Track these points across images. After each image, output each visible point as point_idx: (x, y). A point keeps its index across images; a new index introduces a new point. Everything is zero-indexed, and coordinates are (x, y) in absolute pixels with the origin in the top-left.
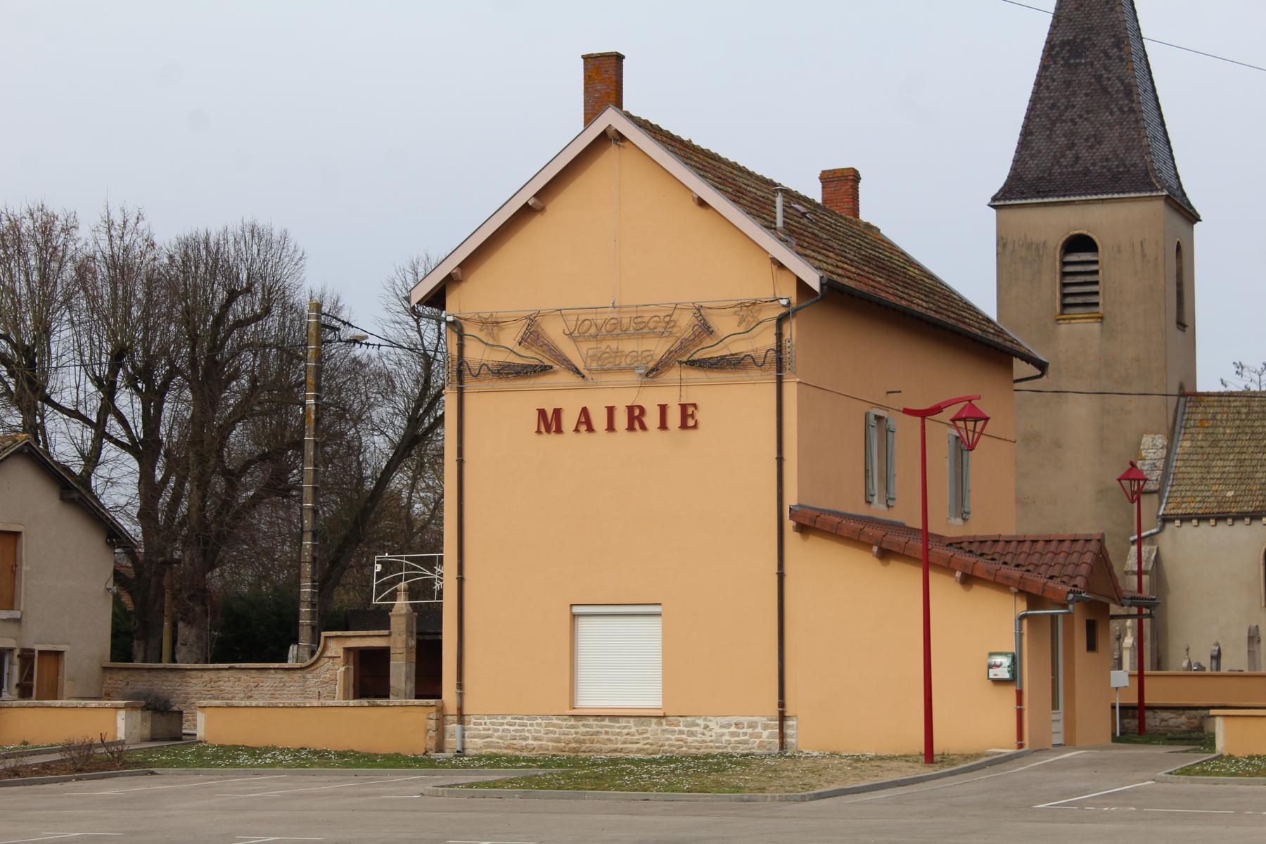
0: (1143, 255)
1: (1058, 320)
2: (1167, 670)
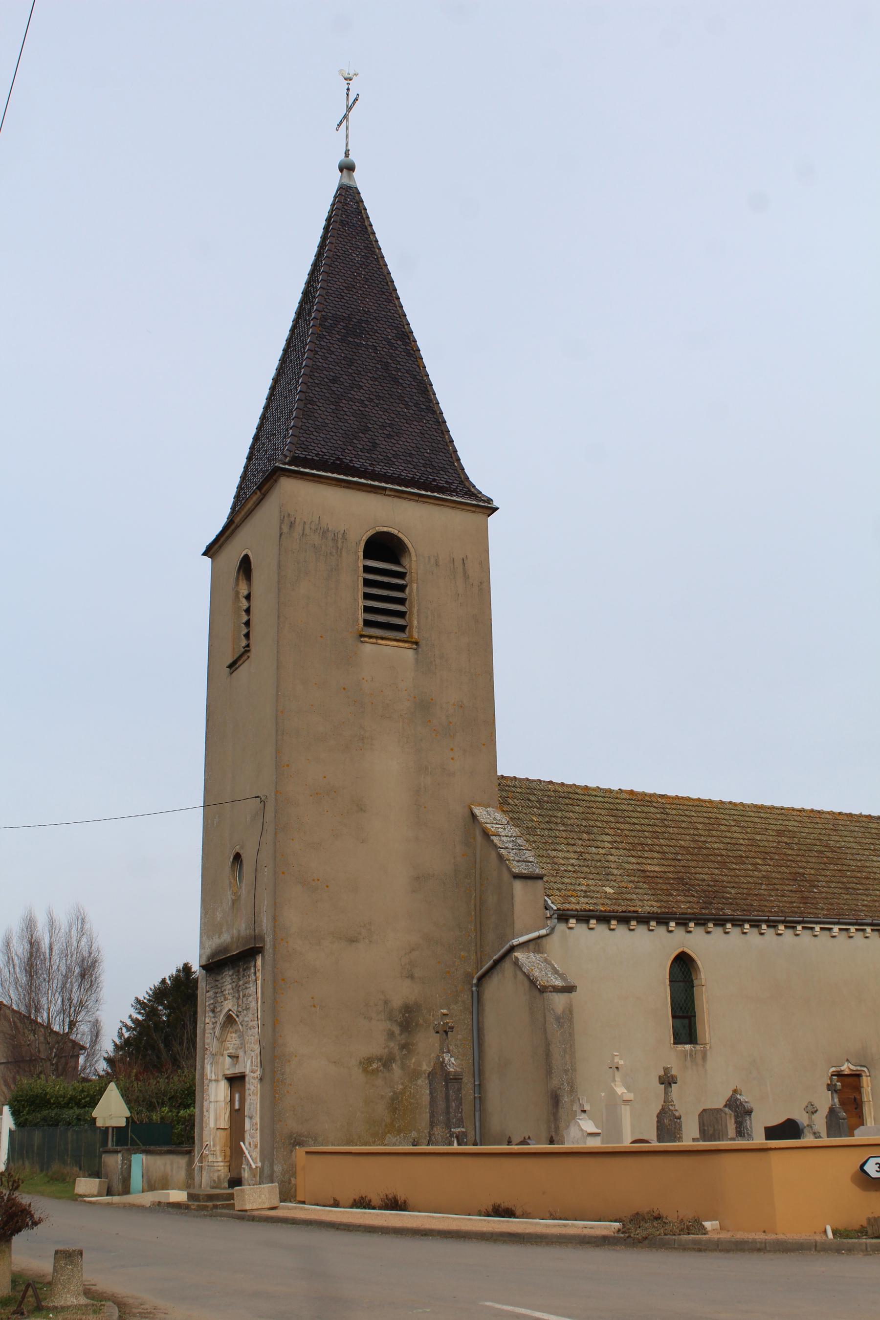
0: (466, 576)
1: (362, 636)
2: (563, 1143)
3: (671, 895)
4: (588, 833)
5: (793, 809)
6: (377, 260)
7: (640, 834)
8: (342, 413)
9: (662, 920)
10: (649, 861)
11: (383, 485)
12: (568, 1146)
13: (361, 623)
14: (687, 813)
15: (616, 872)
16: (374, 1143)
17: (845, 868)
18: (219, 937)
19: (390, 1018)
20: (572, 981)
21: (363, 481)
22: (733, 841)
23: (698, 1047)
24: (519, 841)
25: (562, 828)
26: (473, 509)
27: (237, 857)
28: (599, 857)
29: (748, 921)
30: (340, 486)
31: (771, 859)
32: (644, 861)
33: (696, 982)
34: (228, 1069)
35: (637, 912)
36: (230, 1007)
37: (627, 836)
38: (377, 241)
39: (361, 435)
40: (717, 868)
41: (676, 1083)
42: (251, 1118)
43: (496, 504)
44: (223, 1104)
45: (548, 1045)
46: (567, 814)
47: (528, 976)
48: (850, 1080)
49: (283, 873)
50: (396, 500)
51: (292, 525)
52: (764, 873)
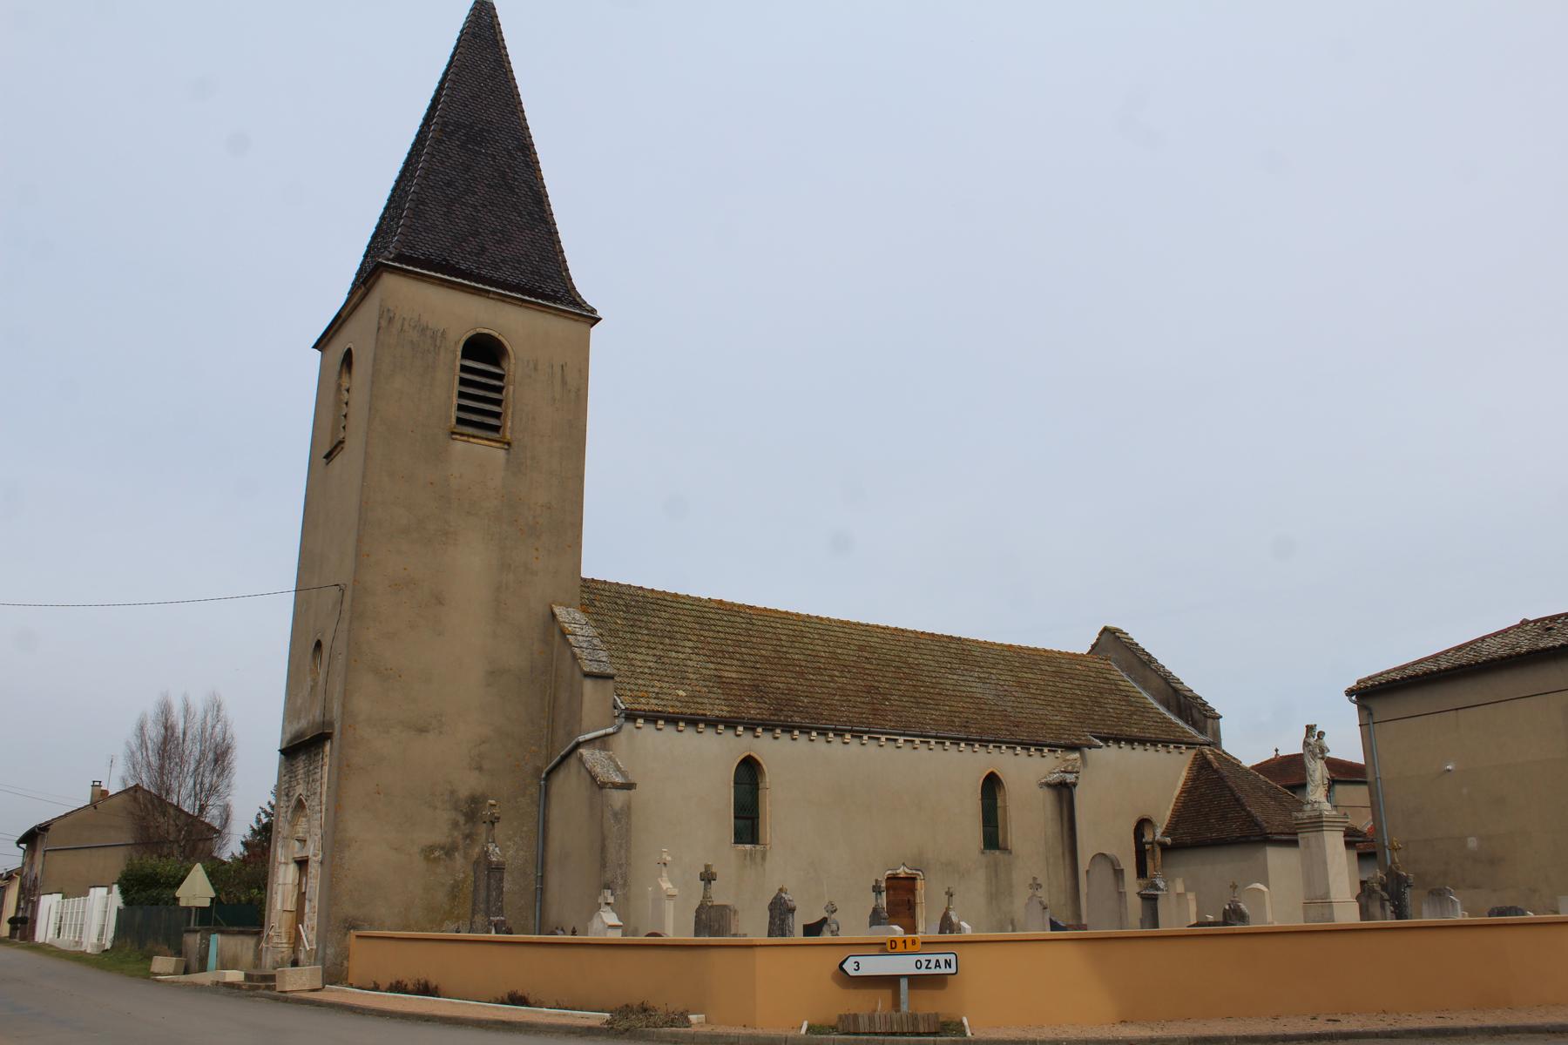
0: (564, 382)
1: (453, 433)
3: (743, 701)
4: (670, 638)
5: (878, 627)
6: (506, 74)
7: (723, 642)
8: (454, 216)
9: (731, 724)
10: (728, 668)
11: (487, 288)
12: (591, 937)
13: (454, 420)
14: (773, 624)
15: (692, 676)
16: (431, 930)
17: (919, 683)
18: (298, 722)
19: (456, 808)
20: (632, 779)
21: (466, 282)
22: (814, 653)
23: (758, 847)
24: (596, 641)
25: (646, 632)
26: (576, 317)
27: (318, 645)
28: (677, 661)
29: (815, 729)
30: (443, 286)
31: (849, 672)
32: (722, 667)
33: (761, 785)
34: (297, 853)
35: (705, 715)
36: (301, 791)
37: (709, 643)
38: (507, 56)
39: (471, 239)
40: (793, 678)
41: (715, 880)
42: (310, 901)
43: (599, 314)
44: (290, 887)
45: (604, 839)
46: (653, 620)
47: (590, 772)
48: (905, 882)
49: (355, 661)
50: (500, 304)
51: (391, 320)
52: (840, 685)
